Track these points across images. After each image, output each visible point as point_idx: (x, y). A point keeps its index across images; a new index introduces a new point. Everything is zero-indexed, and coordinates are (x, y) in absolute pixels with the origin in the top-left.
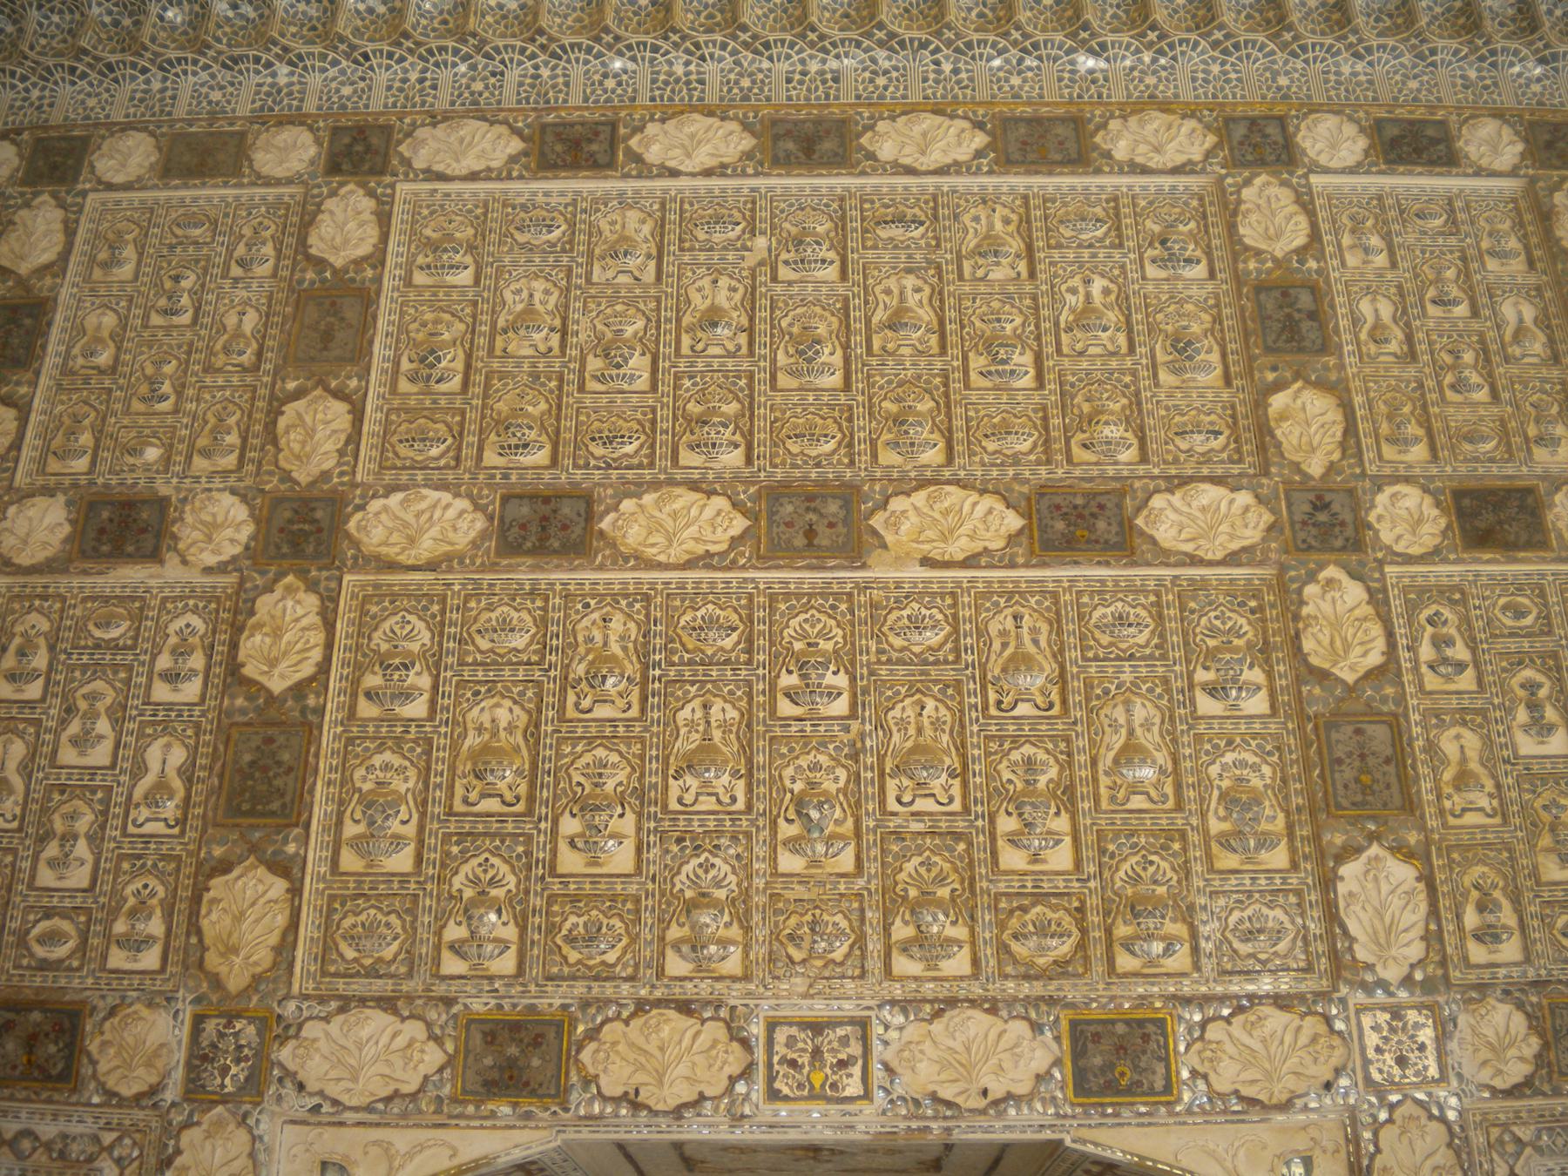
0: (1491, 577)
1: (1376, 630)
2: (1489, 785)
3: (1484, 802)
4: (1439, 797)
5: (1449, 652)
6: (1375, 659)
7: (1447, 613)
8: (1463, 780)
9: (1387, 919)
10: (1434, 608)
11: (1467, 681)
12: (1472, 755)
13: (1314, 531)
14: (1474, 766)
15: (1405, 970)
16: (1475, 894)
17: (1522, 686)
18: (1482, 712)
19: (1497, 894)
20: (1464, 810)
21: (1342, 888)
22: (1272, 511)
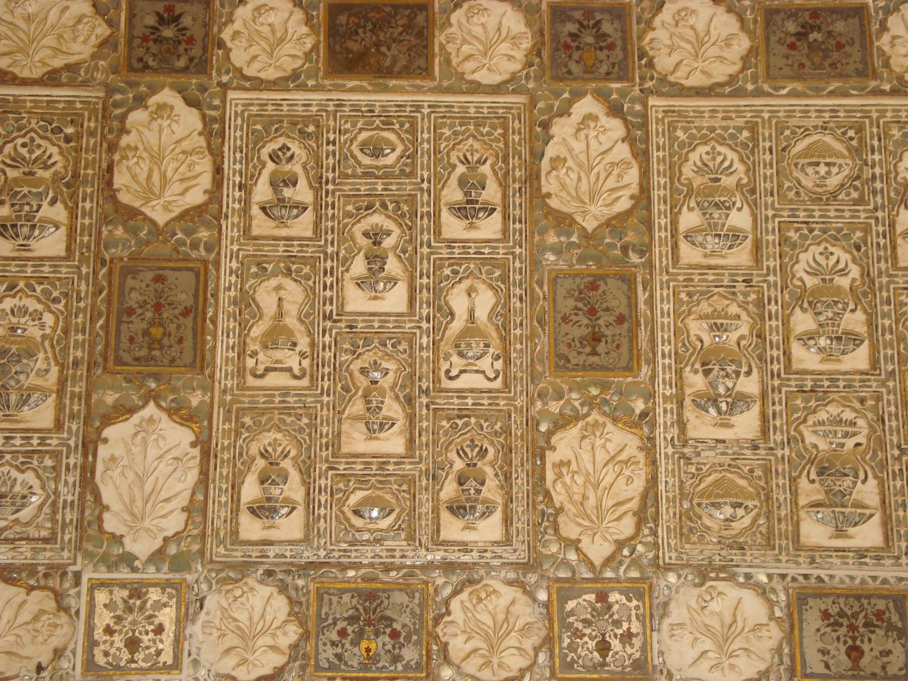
0: (356, 108)
1: (205, 165)
2: (303, 343)
3: (293, 361)
4: (241, 355)
5: (287, 192)
6: (196, 197)
7: (295, 147)
8: (277, 336)
9: (148, 487)
10: (282, 141)
11: (303, 225)
12: (292, 309)
13: (154, 48)
14: (291, 321)
15: (158, 543)
16: (261, 463)
17: (366, 234)
18: (312, 262)
19: (287, 464)
20: (267, 370)
21: (103, 452)
22: (110, 23)
